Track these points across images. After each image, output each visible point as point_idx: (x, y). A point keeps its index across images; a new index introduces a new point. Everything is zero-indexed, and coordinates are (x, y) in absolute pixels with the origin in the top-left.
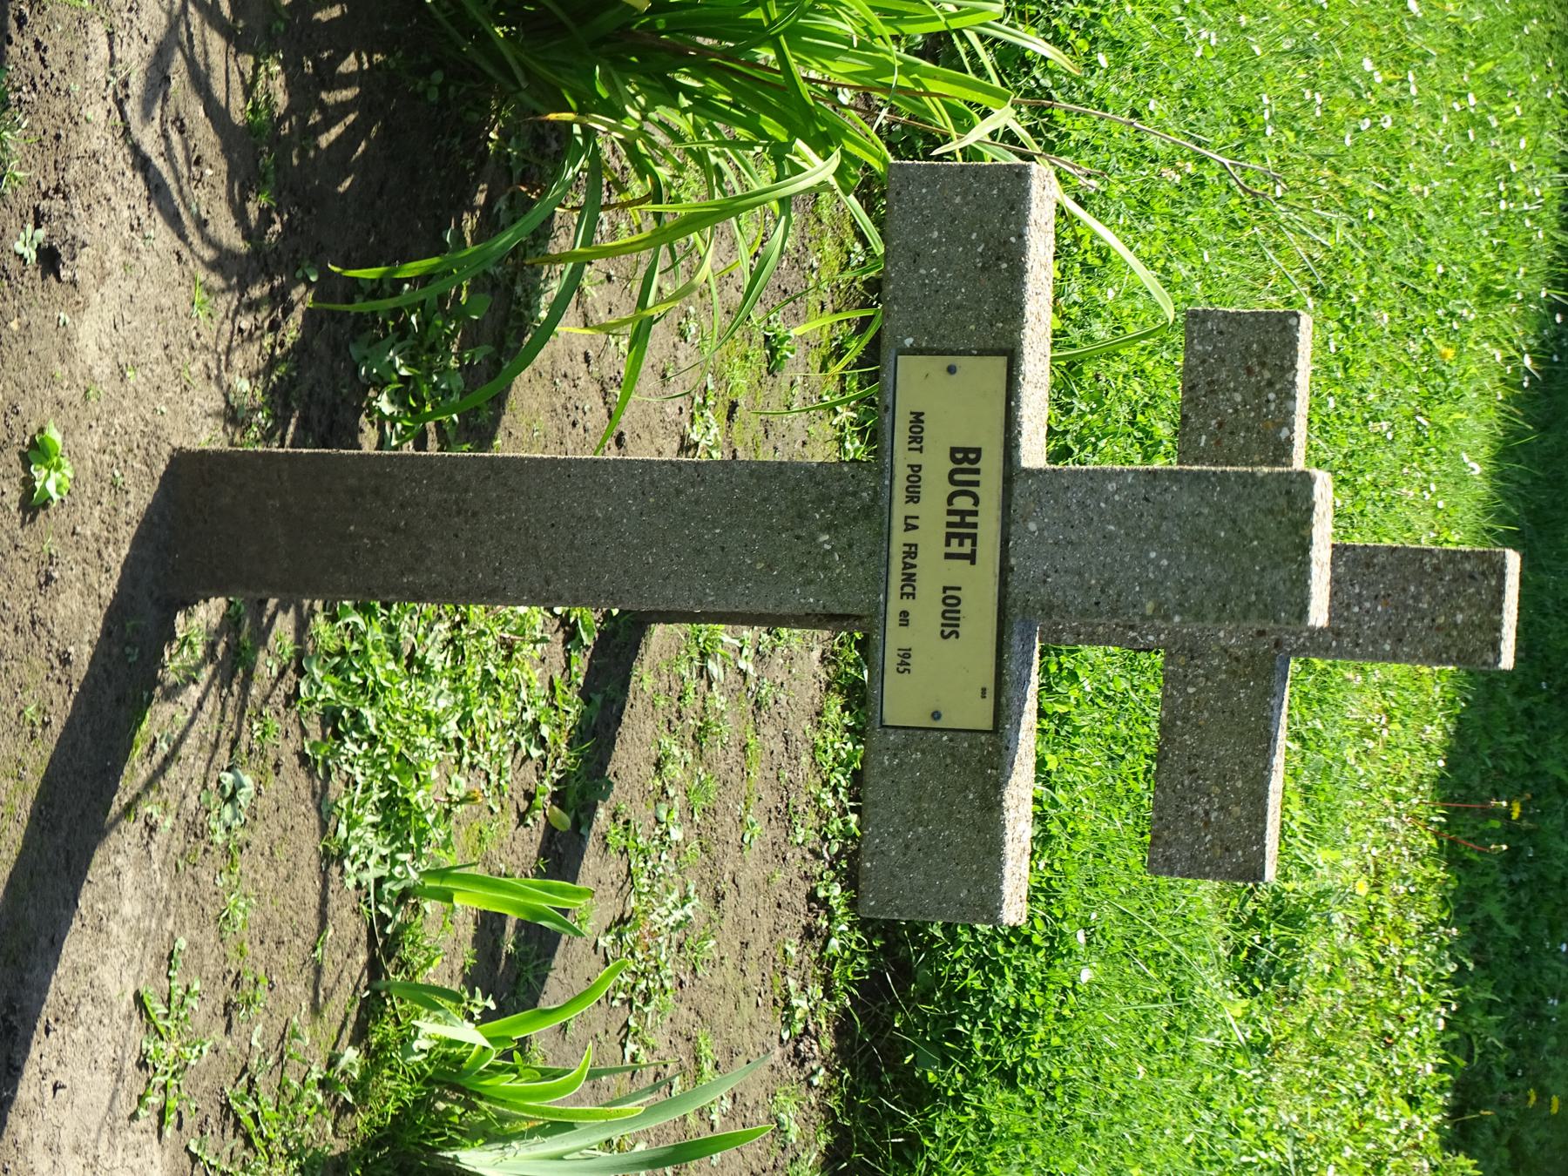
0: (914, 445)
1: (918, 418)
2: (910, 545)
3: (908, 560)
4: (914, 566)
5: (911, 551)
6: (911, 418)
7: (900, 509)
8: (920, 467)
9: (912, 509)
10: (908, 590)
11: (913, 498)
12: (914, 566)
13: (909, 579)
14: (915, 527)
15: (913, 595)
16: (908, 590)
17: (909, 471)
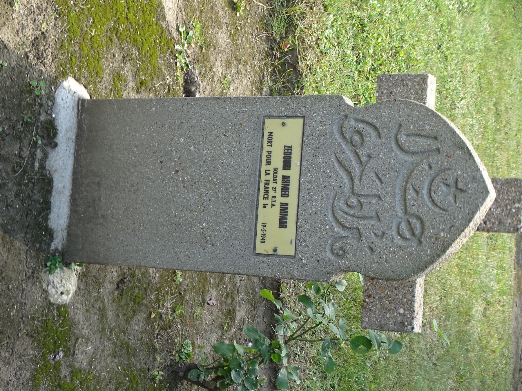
0: (269, 144)
1: (271, 134)
2: (267, 180)
3: (266, 186)
4: (268, 188)
5: (267, 183)
6: (268, 134)
7: (264, 167)
8: (271, 152)
9: (268, 168)
10: (266, 196)
11: (268, 163)
12: (268, 188)
13: (266, 192)
14: (269, 174)
15: (268, 198)
16: (266, 196)
17: (267, 154)
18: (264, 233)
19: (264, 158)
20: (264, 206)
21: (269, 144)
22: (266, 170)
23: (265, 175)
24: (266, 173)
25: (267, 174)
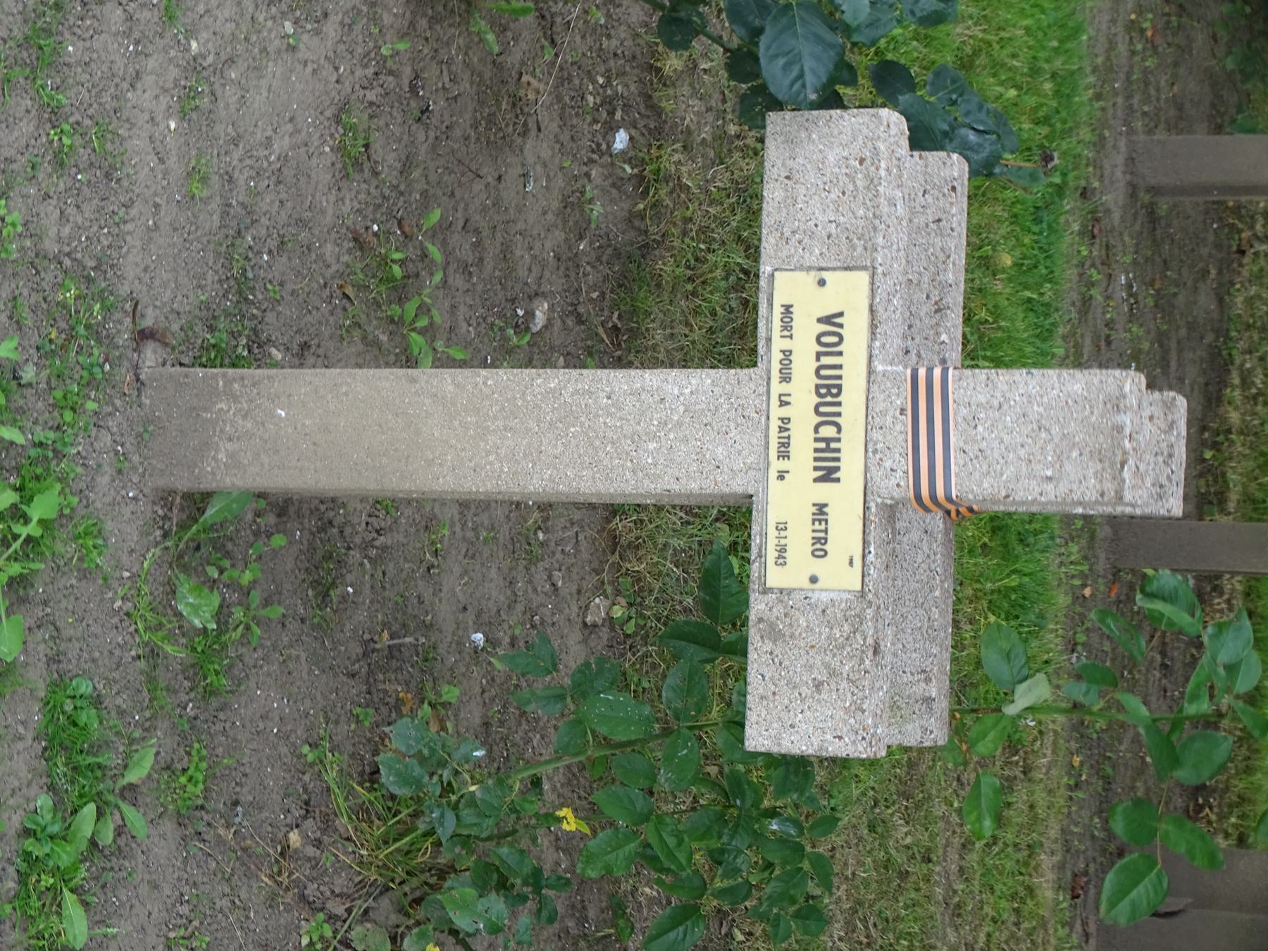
0: (786, 333)
1: (788, 309)
7: (777, 388)
8: (791, 352)
9: (785, 388)
11: (786, 379)
14: (788, 403)
17: (781, 356)
18: (783, 542)
19: (776, 367)
20: (781, 478)
21: (788, 333)
22: (780, 395)
23: (781, 405)
24: (781, 401)
25: (783, 404)
